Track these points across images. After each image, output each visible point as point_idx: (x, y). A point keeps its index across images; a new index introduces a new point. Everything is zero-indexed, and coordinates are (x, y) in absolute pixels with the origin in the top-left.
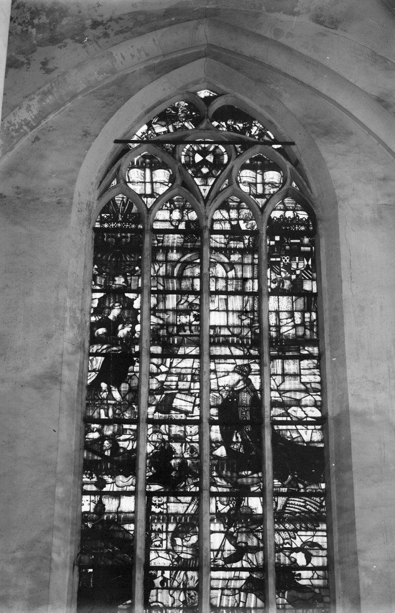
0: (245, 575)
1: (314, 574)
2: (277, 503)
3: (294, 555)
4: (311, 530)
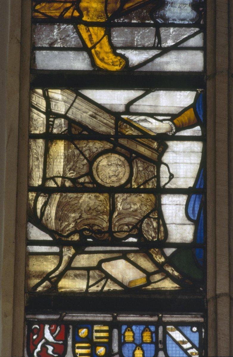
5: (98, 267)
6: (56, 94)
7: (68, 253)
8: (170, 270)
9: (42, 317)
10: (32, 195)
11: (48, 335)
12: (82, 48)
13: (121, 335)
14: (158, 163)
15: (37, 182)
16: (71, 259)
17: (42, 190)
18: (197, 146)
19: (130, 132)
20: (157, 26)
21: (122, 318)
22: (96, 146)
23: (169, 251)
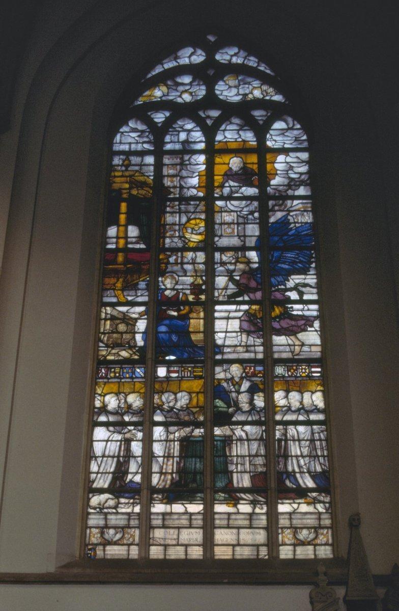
0: (245, 307)
1: (304, 307)
5: (118, 353)
6: (108, 308)
7: (110, 349)
8: (137, 353)
9: (102, 366)
10: (100, 335)
11: (103, 371)
12: (115, 296)
13: (123, 371)
14: (135, 325)
15: (102, 330)
16: (110, 351)
17: (104, 333)
18: (146, 321)
19: (127, 318)
21: (124, 366)
22: (118, 321)
23: (137, 348)
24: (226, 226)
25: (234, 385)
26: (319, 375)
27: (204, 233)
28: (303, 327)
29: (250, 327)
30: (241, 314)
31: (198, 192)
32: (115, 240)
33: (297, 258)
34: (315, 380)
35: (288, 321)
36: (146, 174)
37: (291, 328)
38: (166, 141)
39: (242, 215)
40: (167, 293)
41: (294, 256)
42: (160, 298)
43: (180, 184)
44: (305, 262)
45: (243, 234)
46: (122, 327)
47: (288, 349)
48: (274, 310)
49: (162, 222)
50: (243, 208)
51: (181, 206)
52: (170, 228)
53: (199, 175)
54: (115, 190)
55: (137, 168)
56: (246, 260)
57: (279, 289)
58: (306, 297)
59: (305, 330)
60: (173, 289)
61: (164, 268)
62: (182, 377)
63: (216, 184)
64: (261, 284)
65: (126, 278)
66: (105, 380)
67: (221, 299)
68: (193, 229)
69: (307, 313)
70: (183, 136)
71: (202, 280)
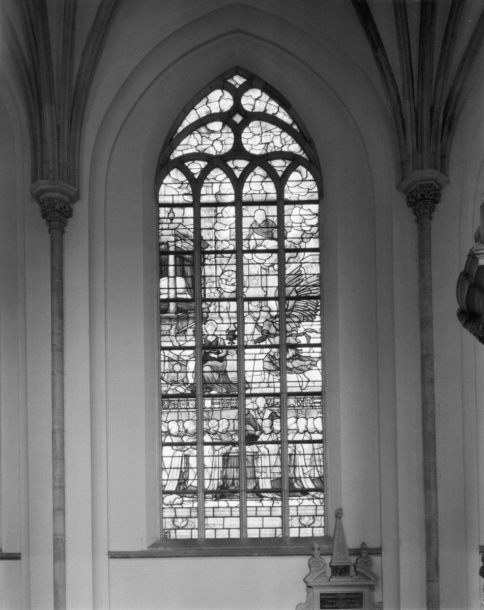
0: (267, 350)
2: (288, 305)
3: (299, 338)
4: (310, 321)
5: (175, 389)
6: (165, 351)
14: (186, 366)
20: (186, 336)
21: (180, 399)
22: (174, 363)
24: (252, 277)
25: (259, 414)
26: (319, 405)
27: (236, 284)
28: (309, 366)
29: (270, 367)
30: (262, 356)
31: (230, 244)
32: (166, 291)
33: (306, 307)
34: (316, 409)
35: (298, 361)
36: (188, 227)
37: (300, 368)
38: (202, 193)
39: (264, 267)
40: (209, 338)
41: (304, 305)
42: (204, 343)
43: (216, 237)
44: (312, 310)
45: (265, 285)
46: (177, 368)
47: (297, 384)
48: (288, 351)
49: (203, 275)
50: (265, 260)
51: (216, 259)
52: (209, 279)
53: (230, 228)
54: (163, 243)
55: (180, 221)
56: (268, 309)
57: (292, 334)
58: (312, 341)
59: (309, 369)
60: (214, 335)
61: (206, 316)
62: (222, 408)
63: (244, 237)
64: (279, 330)
65: (177, 325)
66: (168, 411)
67: (250, 343)
68: (226, 280)
69: (312, 355)
70: (216, 188)
71: (235, 326)
